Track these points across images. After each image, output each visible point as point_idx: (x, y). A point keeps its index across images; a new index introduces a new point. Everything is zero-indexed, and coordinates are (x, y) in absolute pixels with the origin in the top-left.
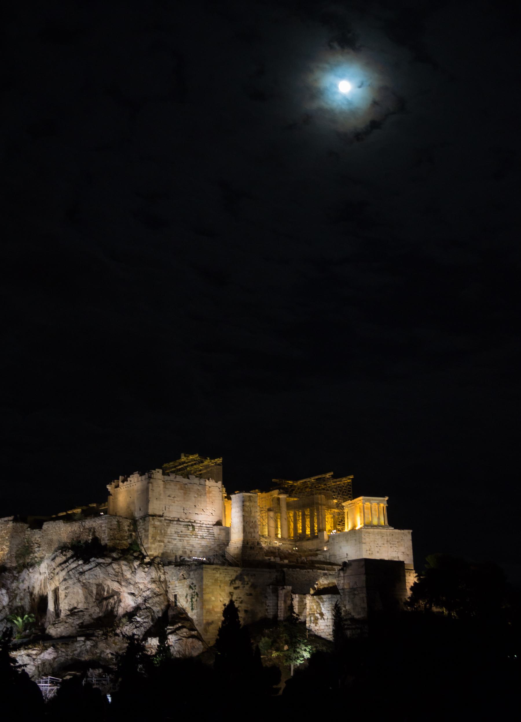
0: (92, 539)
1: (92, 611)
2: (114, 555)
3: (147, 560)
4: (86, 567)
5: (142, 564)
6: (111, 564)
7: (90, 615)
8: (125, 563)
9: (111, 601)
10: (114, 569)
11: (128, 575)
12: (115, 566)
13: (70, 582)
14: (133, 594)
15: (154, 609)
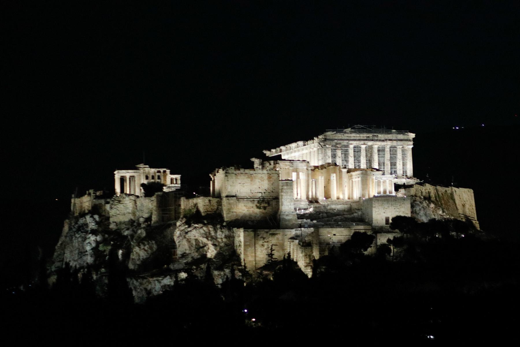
0: (196, 211)
1: (193, 255)
2: (206, 222)
3: (225, 224)
4: (189, 229)
5: (222, 227)
6: (202, 227)
7: (192, 257)
8: (211, 226)
9: (205, 248)
10: (204, 230)
11: (213, 233)
12: (205, 228)
13: (181, 238)
14: (214, 245)
15: (224, 253)
